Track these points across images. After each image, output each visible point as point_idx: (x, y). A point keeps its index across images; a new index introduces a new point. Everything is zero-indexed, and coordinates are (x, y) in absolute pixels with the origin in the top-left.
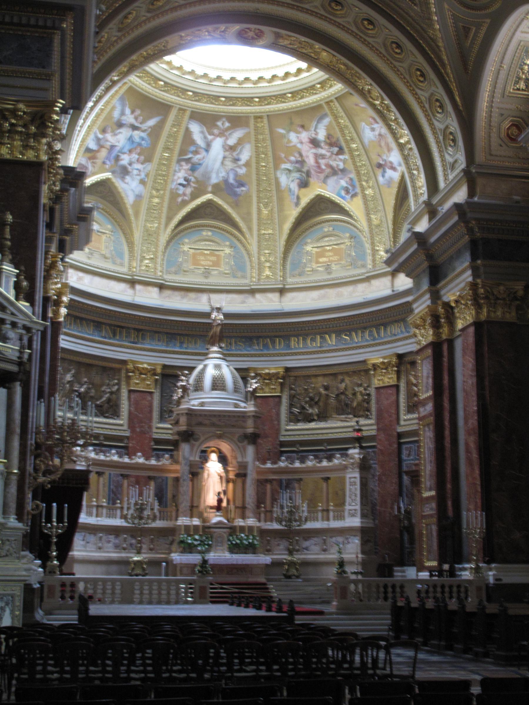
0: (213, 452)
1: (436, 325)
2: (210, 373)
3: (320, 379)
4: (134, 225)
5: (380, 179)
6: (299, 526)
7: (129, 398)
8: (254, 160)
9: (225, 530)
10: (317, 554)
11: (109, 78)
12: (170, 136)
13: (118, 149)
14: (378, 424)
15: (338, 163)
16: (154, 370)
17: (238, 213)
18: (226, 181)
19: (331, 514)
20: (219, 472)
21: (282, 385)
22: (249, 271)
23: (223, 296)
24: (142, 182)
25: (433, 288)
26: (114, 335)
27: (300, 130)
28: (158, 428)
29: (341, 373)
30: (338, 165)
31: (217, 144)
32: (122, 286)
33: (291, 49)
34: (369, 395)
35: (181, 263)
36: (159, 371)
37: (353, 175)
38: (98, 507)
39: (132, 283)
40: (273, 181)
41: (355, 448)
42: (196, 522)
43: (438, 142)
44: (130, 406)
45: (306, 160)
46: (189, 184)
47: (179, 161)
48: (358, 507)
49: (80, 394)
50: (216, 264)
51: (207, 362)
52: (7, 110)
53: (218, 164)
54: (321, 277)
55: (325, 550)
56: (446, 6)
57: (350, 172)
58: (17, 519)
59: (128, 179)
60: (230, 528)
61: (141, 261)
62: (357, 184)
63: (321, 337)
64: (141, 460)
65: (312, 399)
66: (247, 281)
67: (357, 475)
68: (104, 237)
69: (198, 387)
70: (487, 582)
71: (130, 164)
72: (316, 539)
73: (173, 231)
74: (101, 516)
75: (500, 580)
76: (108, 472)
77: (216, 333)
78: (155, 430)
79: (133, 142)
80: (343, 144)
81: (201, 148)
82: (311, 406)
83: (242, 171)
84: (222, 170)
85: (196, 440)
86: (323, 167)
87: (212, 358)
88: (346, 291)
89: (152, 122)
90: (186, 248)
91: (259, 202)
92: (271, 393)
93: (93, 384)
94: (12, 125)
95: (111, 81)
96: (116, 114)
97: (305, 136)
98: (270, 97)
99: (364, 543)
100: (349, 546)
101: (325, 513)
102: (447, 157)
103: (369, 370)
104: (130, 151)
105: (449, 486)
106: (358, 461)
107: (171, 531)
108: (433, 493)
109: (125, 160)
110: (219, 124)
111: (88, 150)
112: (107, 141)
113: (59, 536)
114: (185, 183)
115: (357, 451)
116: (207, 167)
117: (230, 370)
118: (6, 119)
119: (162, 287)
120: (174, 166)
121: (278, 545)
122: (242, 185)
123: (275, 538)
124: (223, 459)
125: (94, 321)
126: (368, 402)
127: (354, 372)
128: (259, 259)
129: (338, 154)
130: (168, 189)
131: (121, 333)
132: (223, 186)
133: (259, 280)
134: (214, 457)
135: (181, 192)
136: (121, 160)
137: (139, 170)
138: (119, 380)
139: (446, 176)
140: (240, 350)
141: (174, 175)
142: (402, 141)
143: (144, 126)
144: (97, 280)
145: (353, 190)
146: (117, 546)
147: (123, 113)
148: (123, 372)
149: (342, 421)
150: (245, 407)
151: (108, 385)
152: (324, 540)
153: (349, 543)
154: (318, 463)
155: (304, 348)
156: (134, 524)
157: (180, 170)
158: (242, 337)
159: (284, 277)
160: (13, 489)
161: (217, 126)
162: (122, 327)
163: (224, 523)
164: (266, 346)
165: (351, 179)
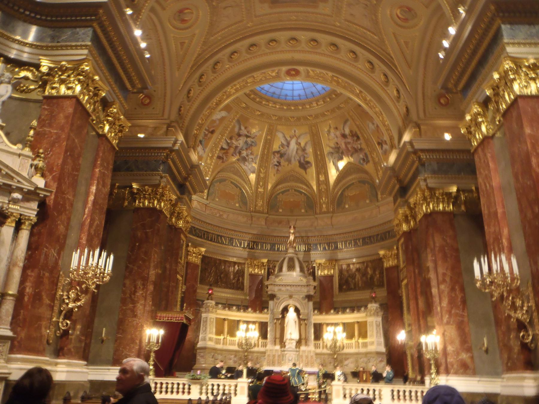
13: (240, 148)
15: (357, 145)
18: (300, 162)
30: (358, 147)
53: (295, 152)
59: (247, 163)
69: (281, 270)
71: (247, 156)
77: (291, 240)
79: (247, 144)
80: (360, 135)
85: (278, 299)
86: (350, 149)
96: (236, 130)
111: (222, 149)
112: (233, 144)
113: (156, 352)
116: (289, 155)
124: (297, 310)
128: (320, 201)
129: (356, 141)
132: (298, 164)
134: (291, 310)
136: (243, 153)
137: (252, 159)
147: (240, 129)
157: (274, 158)
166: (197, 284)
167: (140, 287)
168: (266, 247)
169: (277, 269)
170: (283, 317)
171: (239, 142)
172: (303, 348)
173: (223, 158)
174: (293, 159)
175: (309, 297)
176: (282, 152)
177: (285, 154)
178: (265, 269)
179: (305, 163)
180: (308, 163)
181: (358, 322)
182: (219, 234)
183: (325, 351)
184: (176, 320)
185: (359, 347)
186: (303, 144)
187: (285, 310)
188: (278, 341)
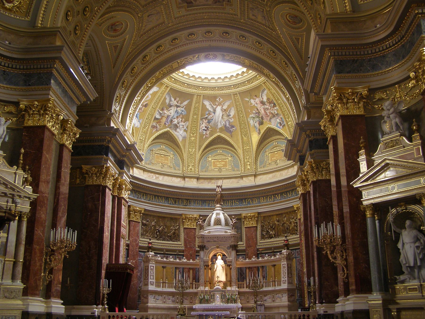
0: (219, 255)
1: (304, 185)
2: (214, 216)
3: (275, 217)
4: (183, 151)
6: (258, 289)
7: (184, 231)
8: (236, 114)
9: (220, 292)
10: (271, 303)
11: (145, 85)
12: (195, 108)
13: (171, 116)
16: (196, 217)
17: (233, 140)
18: (225, 126)
19: (276, 283)
20: (222, 264)
21: (257, 220)
22: (240, 167)
24: (185, 131)
26: (175, 202)
27: (255, 98)
29: (285, 213)
30: (275, 112)
31: (219, 109)
32: (179, 179)
33: (231, 60)
34: (297, 223)
35: (208, 166)
36: (198, 217)
37: (281, 116)
38: (163, 283)
39: (184, 178)
40: (247, 123)
41: (285, 249)
42: (207, 289)
44: (184, 235)
45: (260, 112)
46: (208, 129)
48: (286, 279)
49: (159, 231)
50: (225, 165)
52: (31, 105)
54: (273, 166)
55: (274, 301)
56: (284, 30)
57: (280, 115)
58: (21, 282)
59: (178, 130)
60: (222, 291)
61: (188, 167)
62: (284, 120)
64: (185, 260)
65: (272, 227)
67: (286, 263)
68: (169, 157)
69: (209, 225)
70: (319, 313)
72: (269, 295)
73: (203, 152)
74: (165, 287)
75: (327, 312)
76: (168, 266)
80: (275, 102)
81: (211, 112)
82: (272, 231)
83: (231, 121)
84: (223, 121)
86: (268, 114)
87: (217, 210)
89: (185, 103)
90: (210, 159)
91: (241, 135)
92: (252, 225)
93: (166, 226)
94: (34, 111)
95: (147, 87)
97: (257, 100)
98: (238, 84)
99: (290, 296)
101: (274, 283)
103: (296, 211)
107: (196, 294)
109: (175, 121)
110: (218, 99)
111: (156, 119)
112: (165, 114)
114: (205, 129)
115: (285, 251)
117: (224, 216)
118: (31, 109)
119: (198, 179)
120: (200, 122)
121: (253, 299)
122: (233, 127)
123: (251, 296)
124: (224, 258)
125: (164, 197)
126: (297, 227)
127: (290, 212)
129: (273, 107)
130: (198, 133)
131: (179, 202)
132: (224, 128)
133: (244, 171)
134: (219, 257)
135: (204, 133)
137: (183, 126)
138: (179, 224)
140: (237, 205)
141: (200, 126)
142: (287, 97)
144: (166, 177)
145: (283, 123)
146: (173, 301)
147: (171, 100)
148: (181, 220)
150: (230, 232)
151: (174, 226)
152: (273, 296)
153: (283, 297)
154: (270, 258)
155: (266, 202)
156: (178, 290)
157: (203, 123)
158: (237, 199)
160: (20, 269)
161: (217, 101)
162: (179, 199)
163: (220, 289)
164: (249, 203)
165: (281, 118)
166: (139, 239)
167: (93, 247)
170: (213, 263)
171: (170, 111)
173: (157, 127)
174: (219, 124)
176: (209, 117)
177: (213, 119)
180: (233, 127)
182: (156, 194)
183: (247, 290)
184: (122, 270)
185: (275, 286)
187: (215, 257)
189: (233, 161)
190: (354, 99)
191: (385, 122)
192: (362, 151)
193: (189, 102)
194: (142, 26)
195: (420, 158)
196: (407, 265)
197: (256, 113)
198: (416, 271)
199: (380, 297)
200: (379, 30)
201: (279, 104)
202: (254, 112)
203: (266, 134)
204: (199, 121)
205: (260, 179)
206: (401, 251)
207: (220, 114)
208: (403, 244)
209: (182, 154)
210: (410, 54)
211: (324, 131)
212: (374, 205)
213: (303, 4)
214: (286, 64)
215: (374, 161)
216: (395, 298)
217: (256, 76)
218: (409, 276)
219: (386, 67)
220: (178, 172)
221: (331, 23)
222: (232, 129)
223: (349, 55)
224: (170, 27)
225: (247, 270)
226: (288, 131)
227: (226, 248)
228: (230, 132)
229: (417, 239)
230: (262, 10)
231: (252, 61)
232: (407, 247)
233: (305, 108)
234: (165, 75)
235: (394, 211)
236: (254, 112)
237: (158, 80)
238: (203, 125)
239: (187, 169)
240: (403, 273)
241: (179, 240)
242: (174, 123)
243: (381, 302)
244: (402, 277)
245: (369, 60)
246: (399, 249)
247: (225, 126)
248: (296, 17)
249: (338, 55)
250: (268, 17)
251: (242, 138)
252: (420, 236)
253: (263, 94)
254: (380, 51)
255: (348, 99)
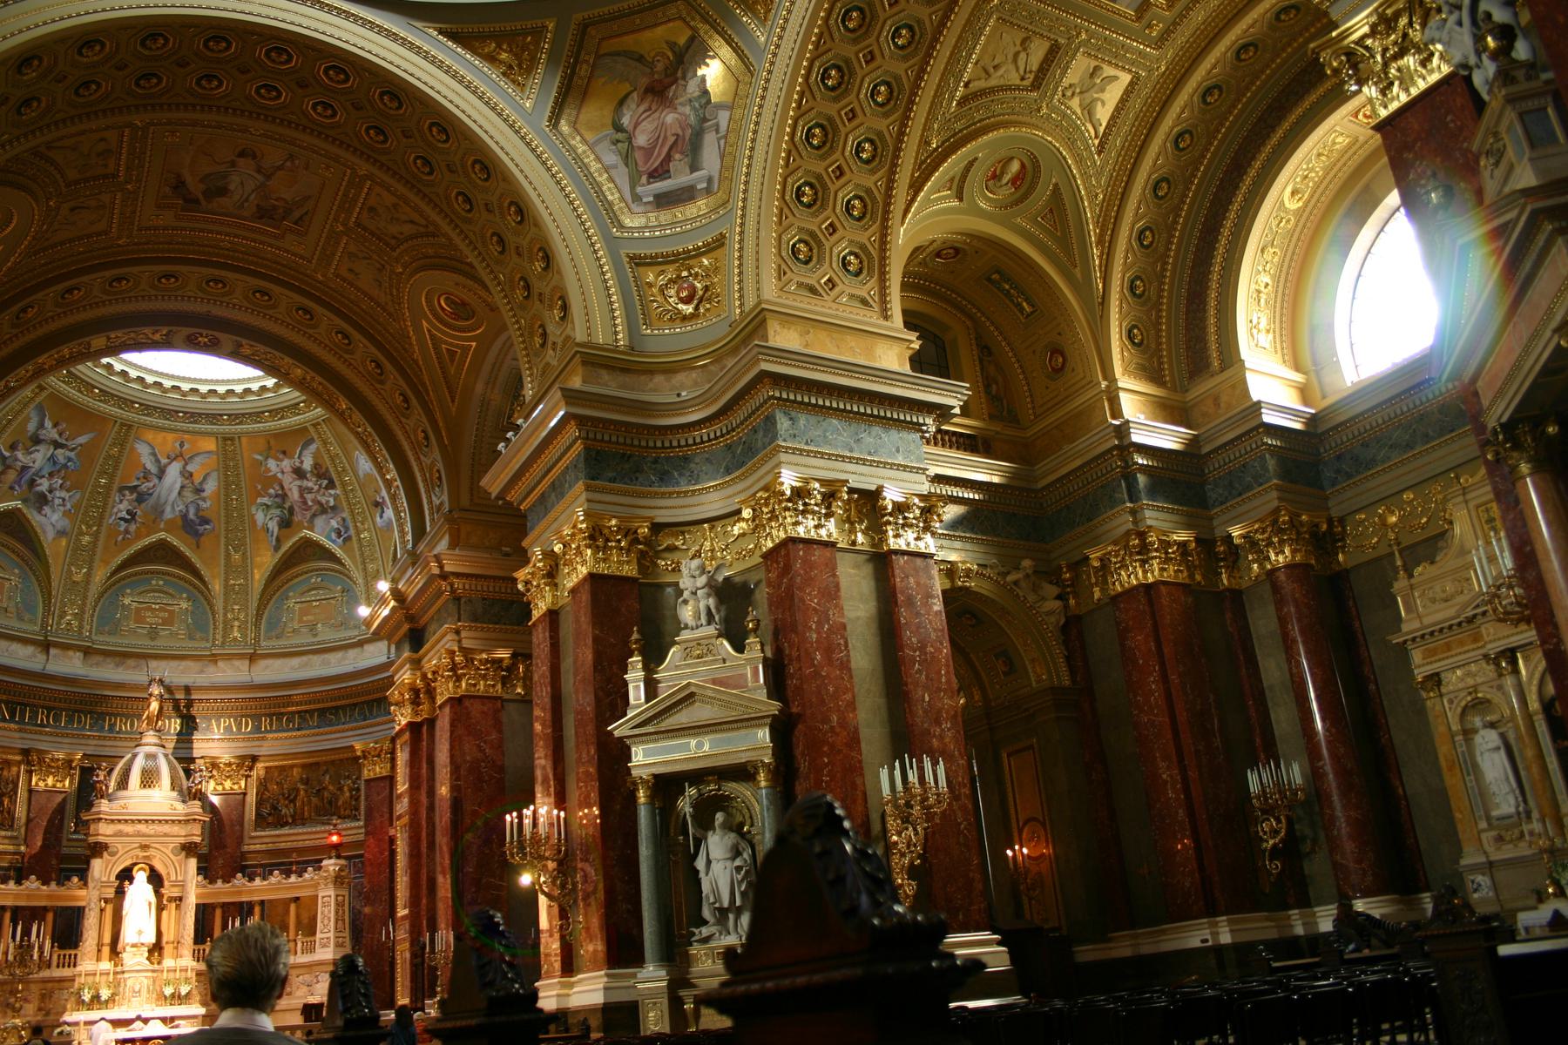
1: (415, 702)
5: (378, 519)
8: (222, 491)
12: (109, 457)
14: (366, 826)
18: (184, 516)
23: (163, 663)
24: (65, 514)
25: (415, 656)
27: (281, 456)
28: (70, 840)
30: (328, 502)
31: (174, 471)
32: (30, 650)
34: (358, 790)
35: (119, 620)
39: (46, 646)
41: (330, 858)
43: (425, 480)
47: (121, 490)
48: (331, 935)
51: (138, 749)
54: (304, 639)
57: (343, 510)
59: (47, 509)
60: (153, 971)
61: (61, 617)
62: (351, 526)
63: (300, 717)
66: (208, 645)
67: (332, 893)
68: (7, 584)
69: (123, 784)
78: (65, 843)
79: (55, 463)
80: (334, 476)
85: (113, 854)
88: (333, 657)
89: (82, 440)
90: (127, 601)
97: (286, 464)
98: (243, 415)
100: (318, 986)
102: (434, 498)
103: (359, 758)
104: (51, 475)
105: (424, 901)
106: (333, 874)
108: (406, 912)
109: (43, 485)
112: (17, 459)
114: (128, 517)
115: (332, 861)
116: (159, 496)
119: (87, 652)
124: (155, 879)
126: (357, 799)
128: (225, 615)
129: (327, 488)
132: (180, 523)
133: (223, 643)
134: (141, 877)
135: (122, 529)
136: (40, 485)
137: (64, 500)
139: (432, 520)
141: (113, 507)
143: (71, 444)
147: (41, 425)
149: (324, 824)
157: (121, 501)
159: (257, 639)
162: (26, 705)
165: (344, 520)
168: (79, 722)
169: (112, 784)
172: (168, 962)
174: (168, 509)
175: (189, 849)
176: (143, 488)
178: (72, 777)
179: (197, 521)
180: (205, 521)
181: (297, 899)
186: (197, 479)
187: (126, 875)
188: (106, 950)
189: (192, 613)
190: (619, 541)
191: (686, 602)
192: (636, 659)
193: (92, 439)
194: (47, 230)
195: (759, 688)
196: (717, 905)
197: (277, 496)
198: (731, 916)
199: (663, 973)
200: (686, 405)
201: (344, 485)
202: (272, 491)
203: (294, 552)
204: (113, 493)
205: (267, 667)
206: (702, 875)
207: (175, 482)
208: (709, 862)
209: (49, 578)
210: (743, 469)
211: (524, 595)
212: (655, 776)
213: (503, 290)
214: (406, 400)
215: (659, 682)
216: (688, 973)
217: (298, 404)
218: (719, 927)
219: (689, 483)
220: (25, 627)
221: (584, 363)
222: (201, 528)
223: (617, 443)
224: (119, 246)
225: (218, 913)
226: (357, 553)
227: (168, 852)
228: (197, 535)
229: (736, 853)
230: (378, 266)
231: (313, 374)
232: (717, 867)
233: (450, 519)
234: (62, 363)
235: (692, 792)
236: (272, 491)
237: (40, 372)
238: (121, 507)
239: (59, 623)
240: (705, 923)
241: (12, 826)
242: (38, 488)
243: (664, 984)
244: (705, 931)
245: (656, 461)
246: (698, 872)
247: (184, 516)
248: (464, 304)
249: (595, 440)
250: (391, 286)
251: (228, 555)
252: (743, 844)
253: (305, 453)
254: (679, 446)
255: (608, 540)
